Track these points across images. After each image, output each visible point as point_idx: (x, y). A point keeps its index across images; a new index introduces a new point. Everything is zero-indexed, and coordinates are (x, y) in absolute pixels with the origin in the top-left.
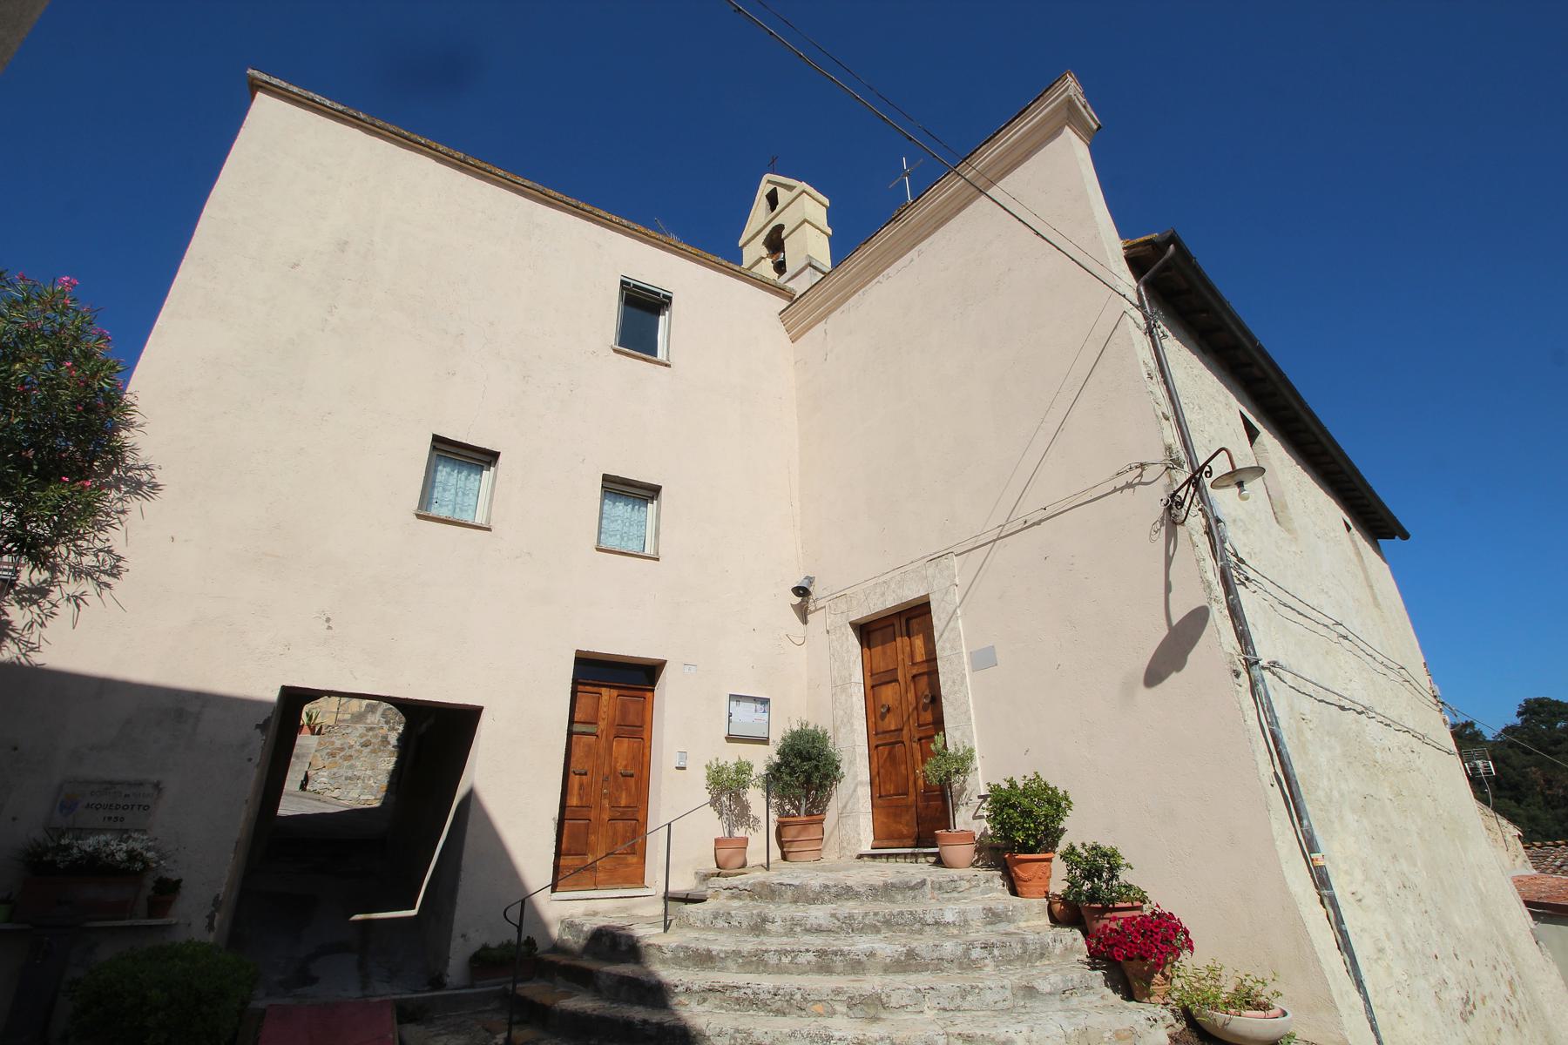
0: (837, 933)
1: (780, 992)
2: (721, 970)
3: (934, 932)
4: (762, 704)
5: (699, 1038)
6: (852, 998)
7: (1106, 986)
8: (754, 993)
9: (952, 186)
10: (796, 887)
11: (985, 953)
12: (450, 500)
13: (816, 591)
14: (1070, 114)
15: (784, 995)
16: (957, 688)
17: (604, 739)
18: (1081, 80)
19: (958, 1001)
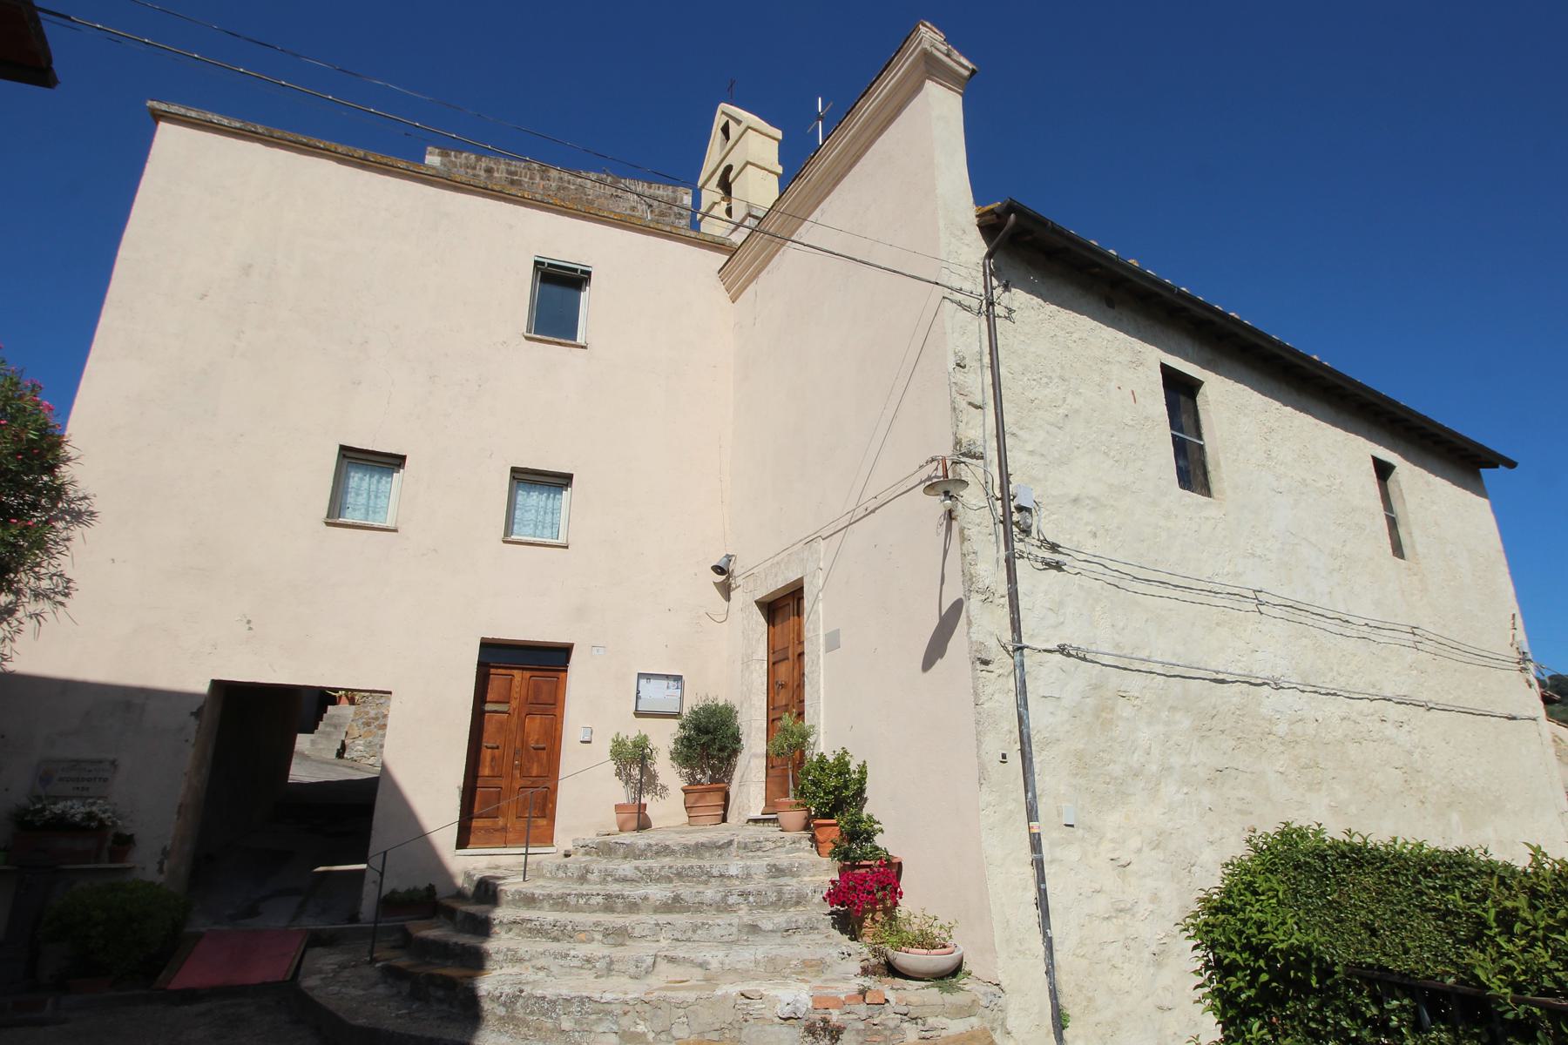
0: (639, 882)
1: (558, 924)
2: (539, 909)
3: (718, 883)
4: (674, 681)
5: (485, 954)
6: (607, 929)
7: (834, 927)
8: (541, 925)
9: (840, 143)
10: (627, 845)
11: (741, 899)
12: (363, 504)
13: (737, 568)
14: (931, 68)
15: (560, 927)
16: (814, 668)
17: (516, 716)
18: (939, 25)
19: (689, 934)
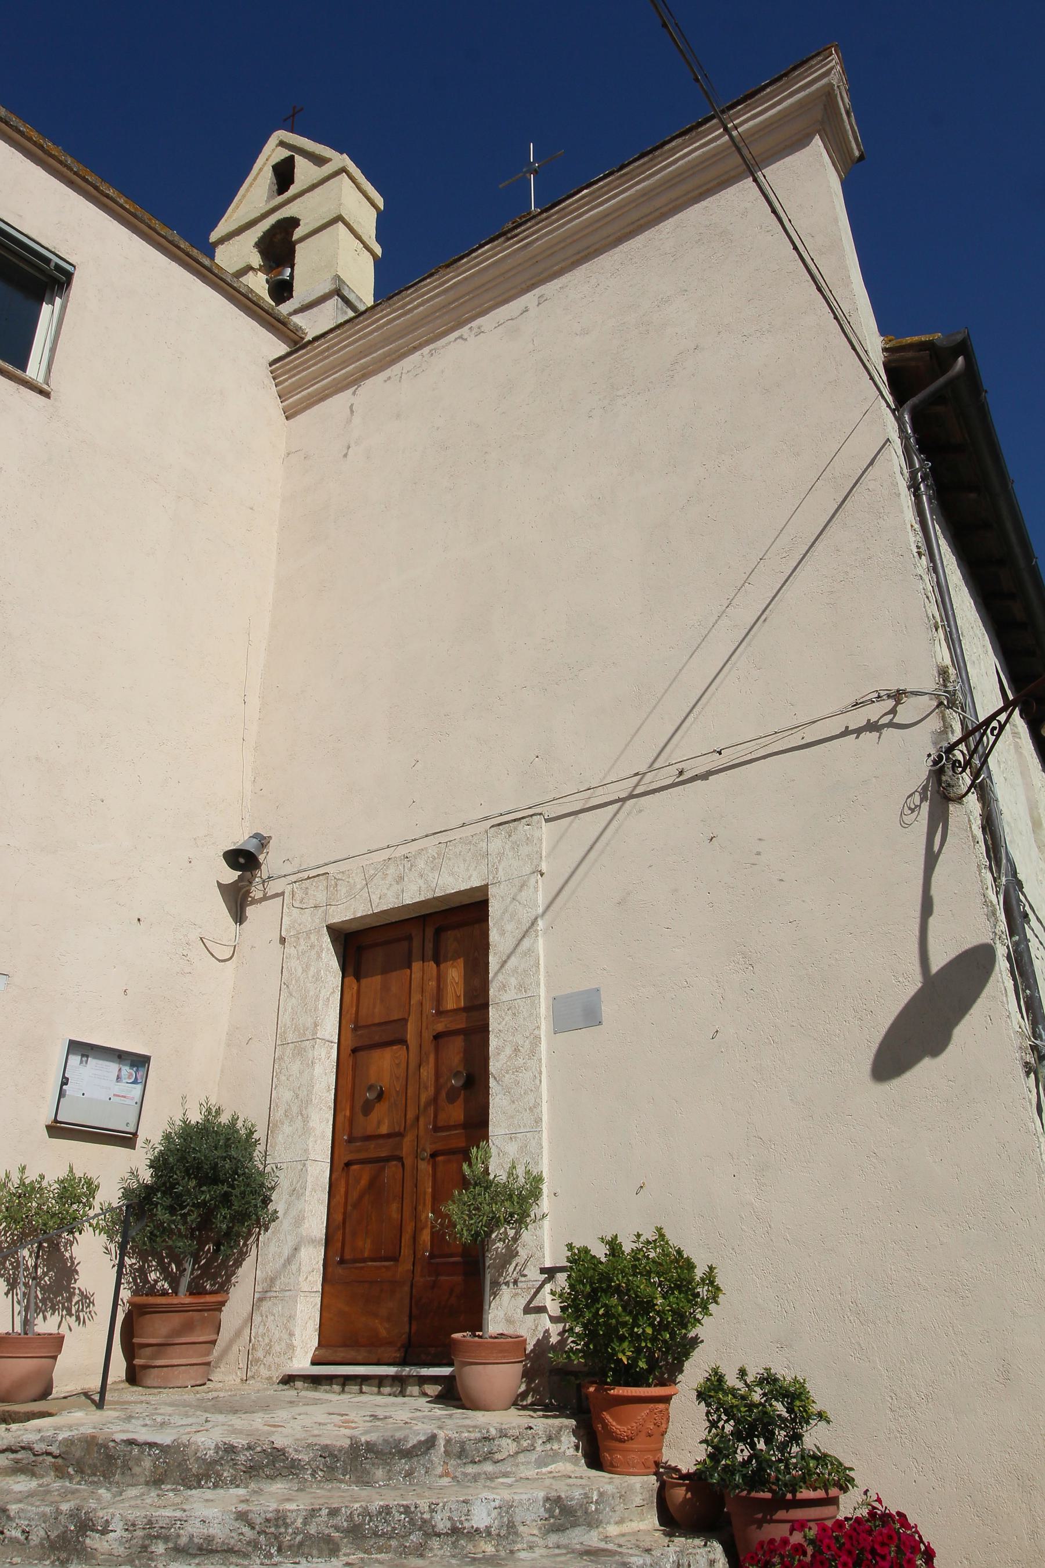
0: (246, 1555)
3: (447, 1550)
4: (132, 1065)
10: (164, 1449)
13: (270, 862)
18: (848, 69)
